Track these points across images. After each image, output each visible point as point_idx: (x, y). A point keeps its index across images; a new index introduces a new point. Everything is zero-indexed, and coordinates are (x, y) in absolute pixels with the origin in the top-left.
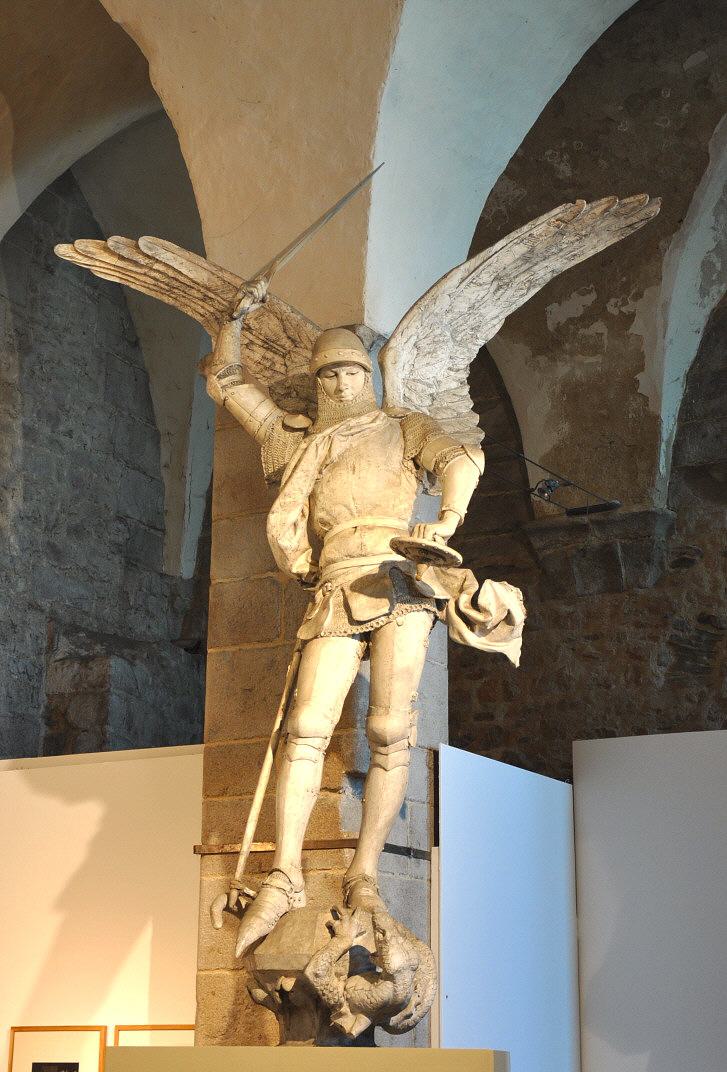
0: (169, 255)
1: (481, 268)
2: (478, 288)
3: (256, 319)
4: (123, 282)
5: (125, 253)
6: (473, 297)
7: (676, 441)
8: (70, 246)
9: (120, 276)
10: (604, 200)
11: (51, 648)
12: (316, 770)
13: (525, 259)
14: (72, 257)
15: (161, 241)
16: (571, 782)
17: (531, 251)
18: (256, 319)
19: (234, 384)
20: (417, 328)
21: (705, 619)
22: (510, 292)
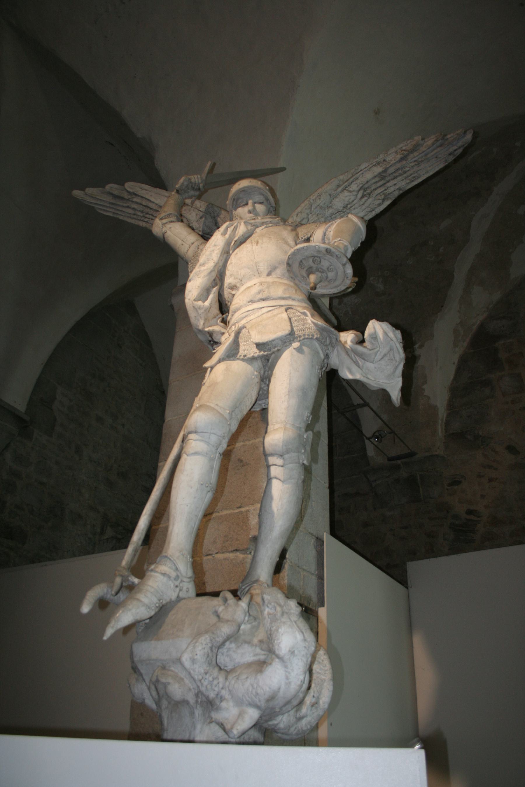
0: (144, 192)
1: (352, 179)
2: (350, 194)
3: (197, 221)
4: (115, 216)
5: (116, 193)
6: (347, 199)
7: (446, 420)
8: (82, 192)
9: (113, 211)
10: (433, 137)
11: (102, 533)
12: (212, 468)
13: (382, 176)
14: (83, 198)
15: (139, 184)
16: (407, 587)
17: (385, 171)
18: (197, 221)
19: (172, 222)
20: (307, 214)
21: (470, 512)
22: (371, 200)
